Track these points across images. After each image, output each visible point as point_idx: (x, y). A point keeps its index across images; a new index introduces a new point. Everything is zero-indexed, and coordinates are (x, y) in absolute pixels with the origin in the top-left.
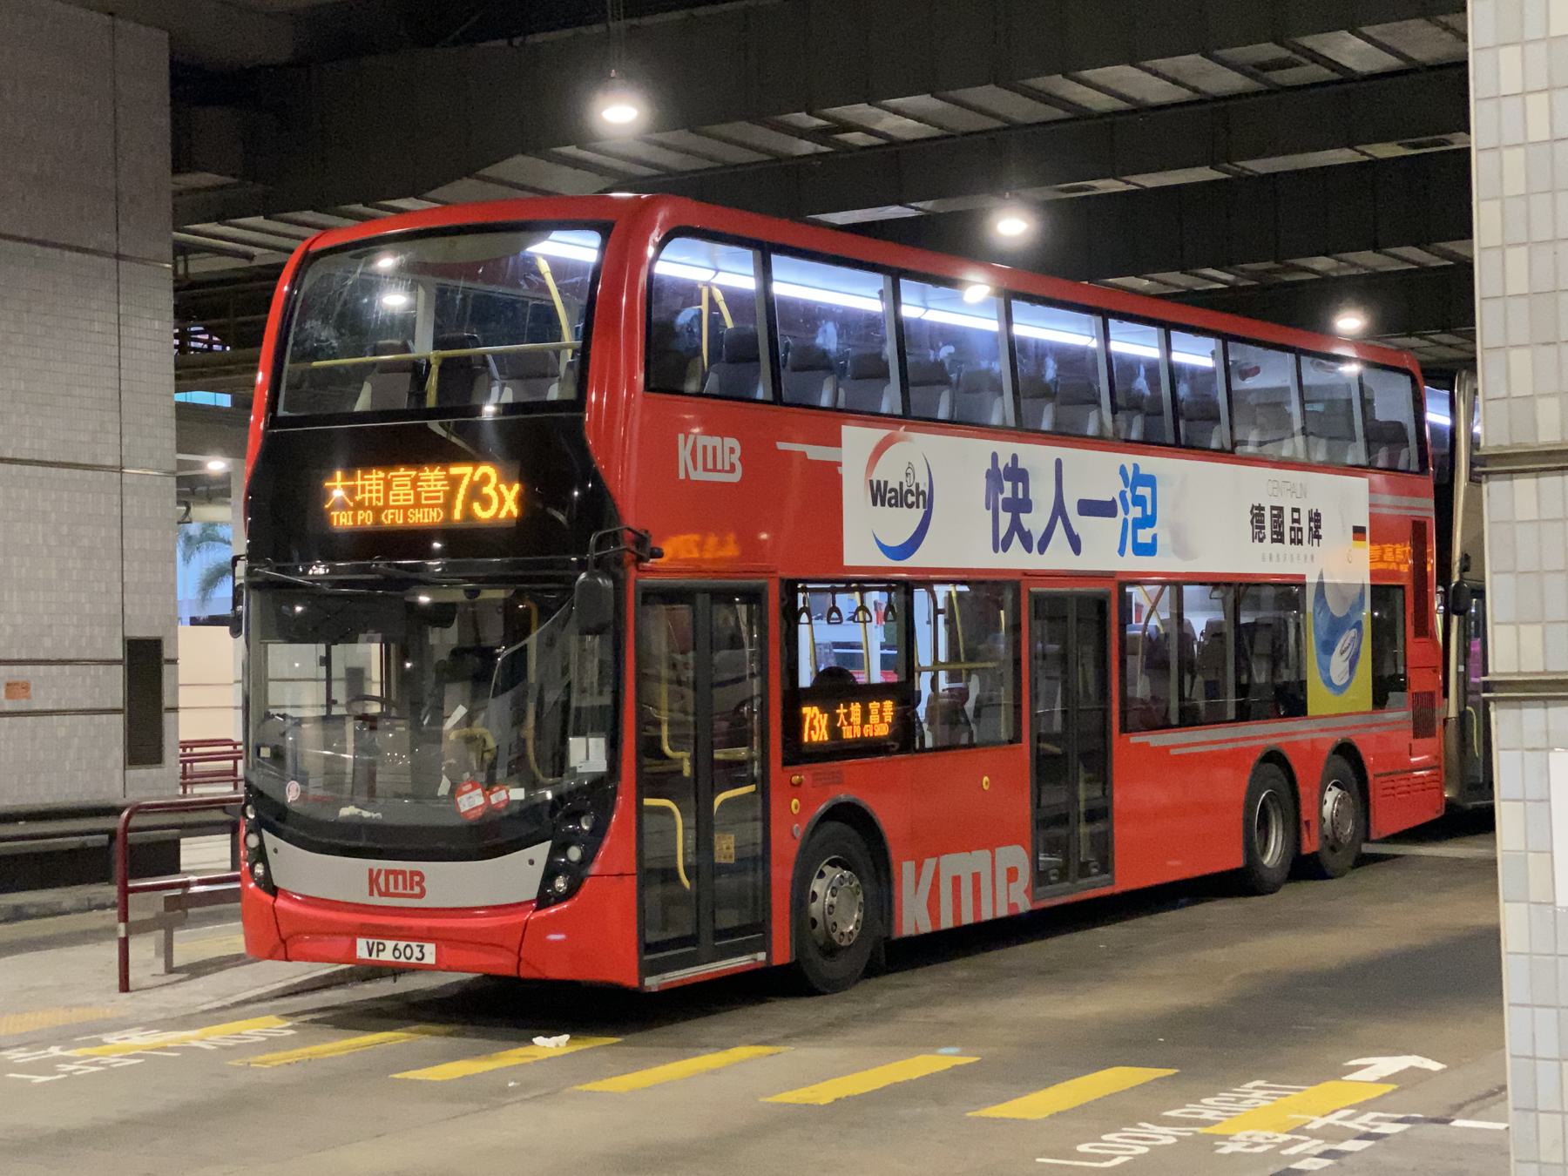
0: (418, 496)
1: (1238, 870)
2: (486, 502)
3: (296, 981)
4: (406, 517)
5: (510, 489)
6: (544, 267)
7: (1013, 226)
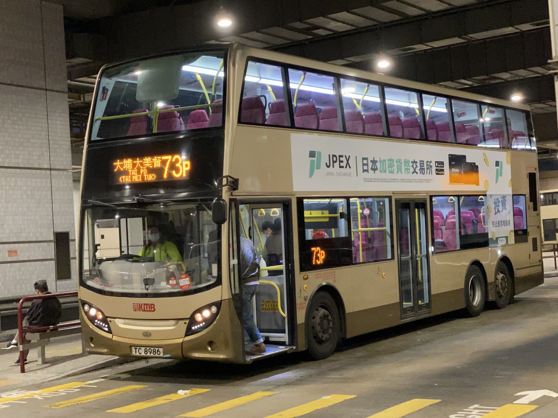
1: (464, 309)
2: (177, 170)
3: (90, 366)
6: (199, 78)
7: (384, 64)
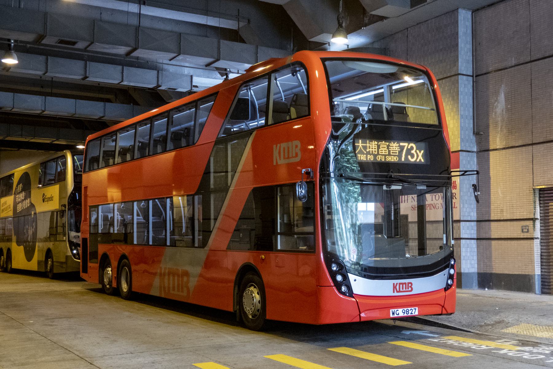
0: (389, 151)
2: (413, 156)
4: (385, 159)
5: (420, 152)
